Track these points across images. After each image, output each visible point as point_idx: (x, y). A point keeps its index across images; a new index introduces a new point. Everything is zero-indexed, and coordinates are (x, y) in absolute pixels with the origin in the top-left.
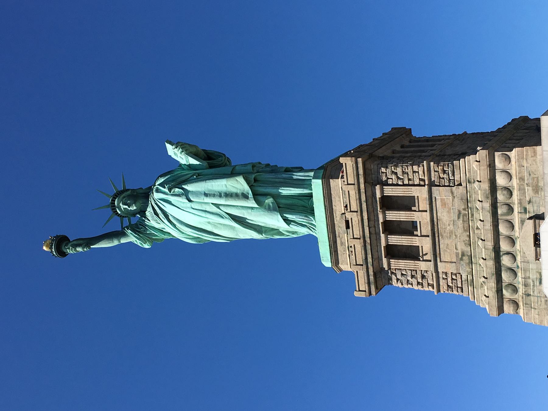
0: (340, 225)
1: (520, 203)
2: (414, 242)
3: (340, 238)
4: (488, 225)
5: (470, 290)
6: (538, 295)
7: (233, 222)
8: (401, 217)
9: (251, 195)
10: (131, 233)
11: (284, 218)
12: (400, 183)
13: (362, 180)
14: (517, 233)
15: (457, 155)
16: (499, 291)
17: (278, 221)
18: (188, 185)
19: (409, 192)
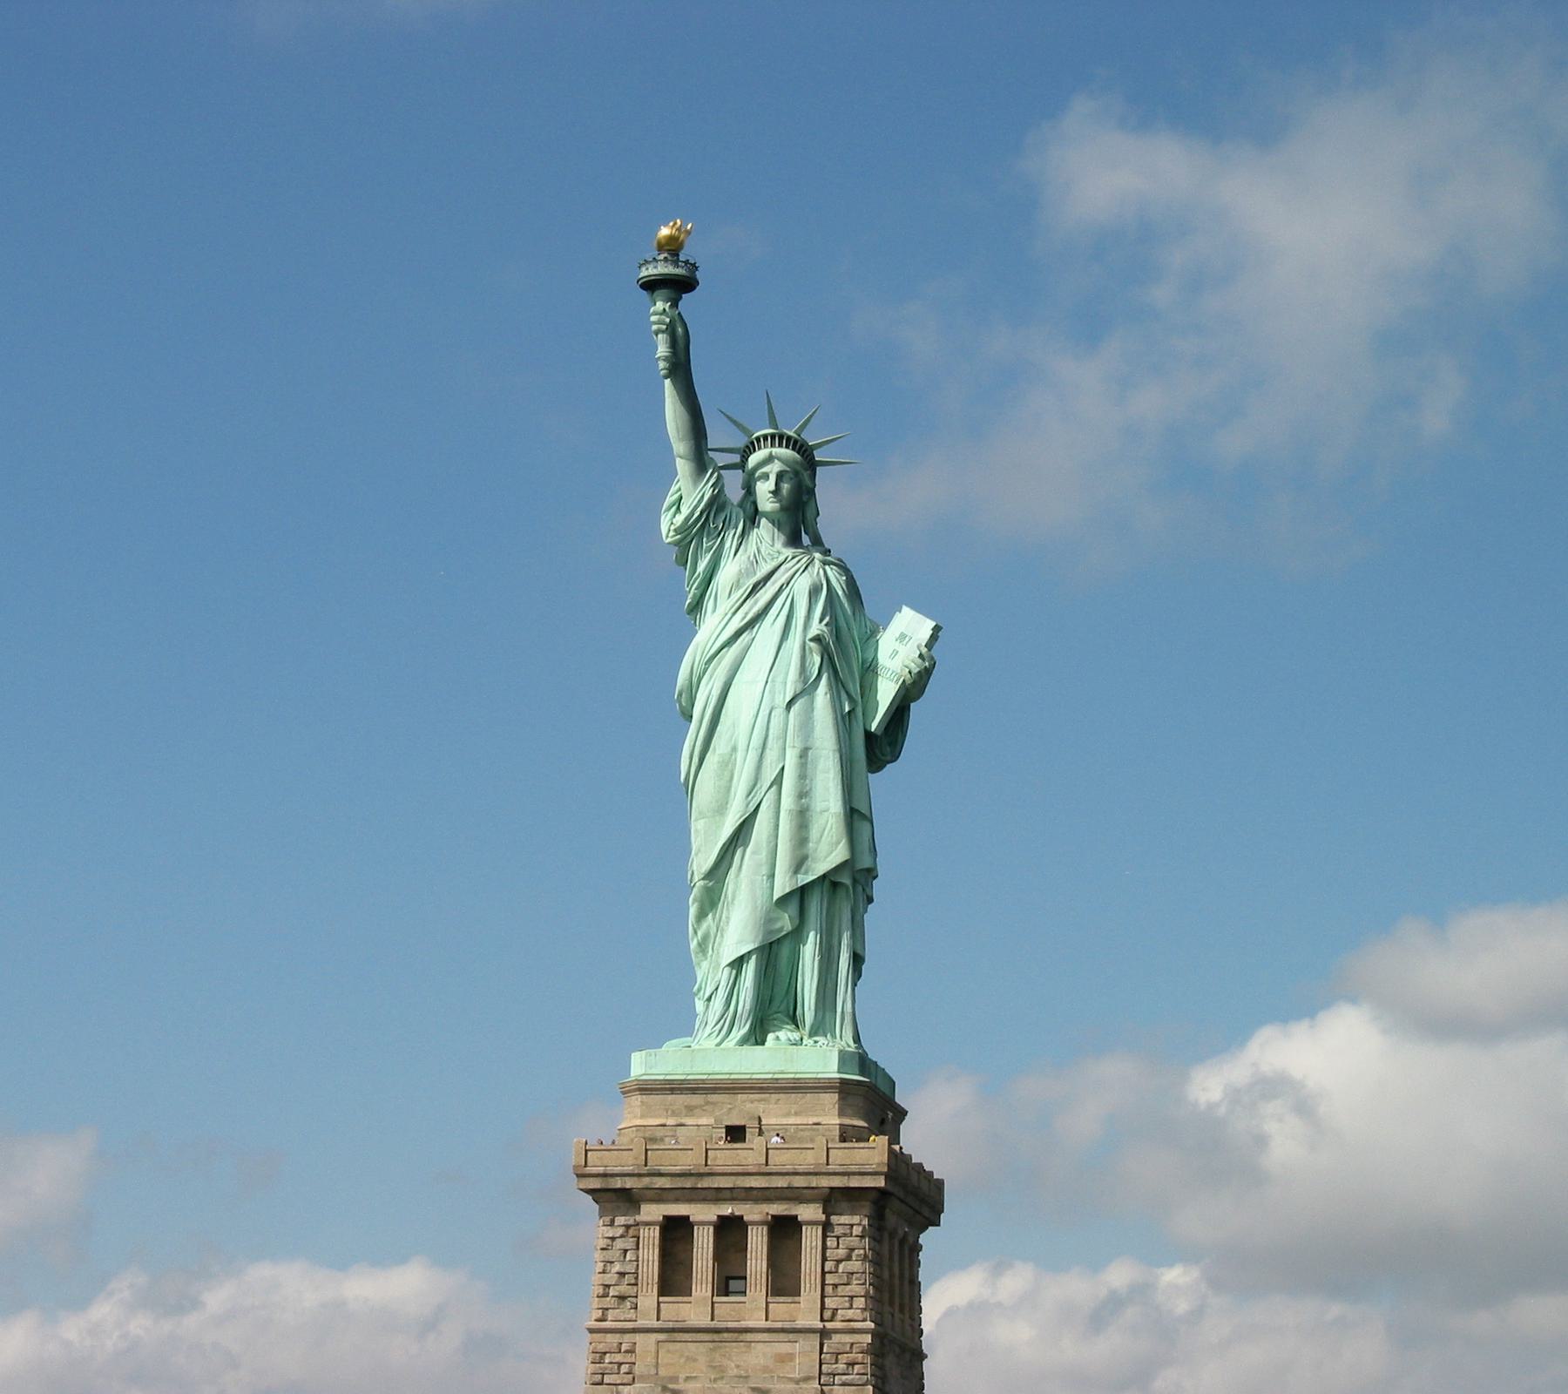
0: (735, 1112)
3: (701, 1106)
7: (736, 822)
8: (754, 1261)
9: (804, 879)
10: (703, 497)
11: (745, 959)
12: (829, 1266)
13: (837, 1182)
15: (883, 1383)
17: (740, 942)
18: (828, 695)
19: (808, 1285)
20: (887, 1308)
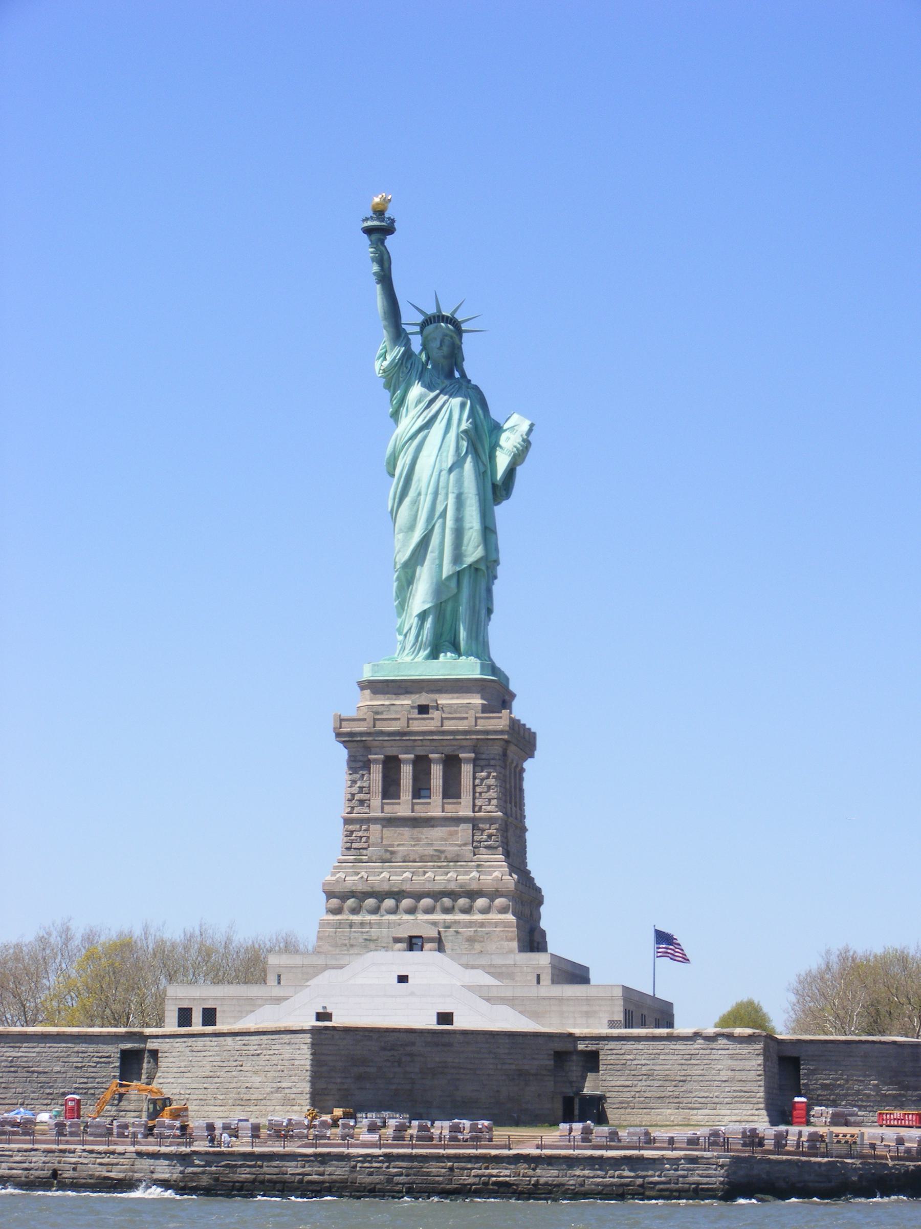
1: (457, 923)
2: (404, 794)
4: (429, 887)
5: (349, 859)
6: (352, 937)
10: (399, 351)
12: (477, 781)
14: (421, 917)
15: (507, 846)
16: (352, 894)
17: (424, 602)
20: (509, 806)
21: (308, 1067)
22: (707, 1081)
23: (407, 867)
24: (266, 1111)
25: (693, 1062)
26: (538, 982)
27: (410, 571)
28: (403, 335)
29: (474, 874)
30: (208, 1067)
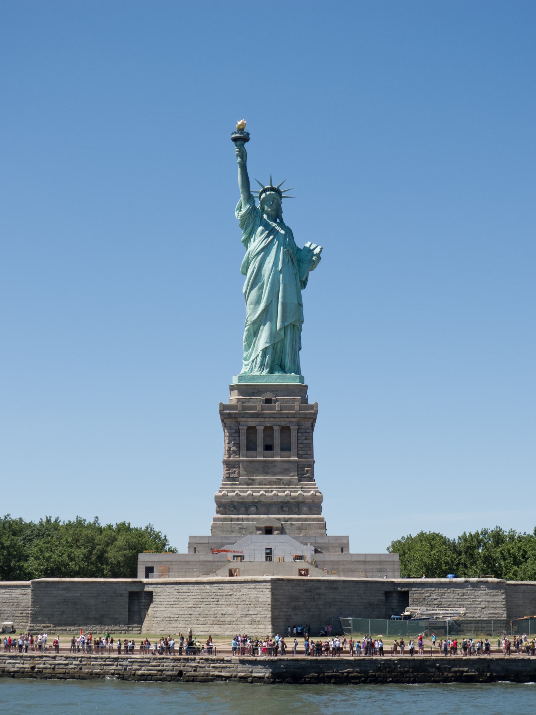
6: (232, 527)
9: (286, 324)
12: (300, 442)
17: (266, 343)
21: (270, 603)
22: (473, 608)
23: (262, 488)
24: (237, 628)
25: (464, 597)
26: (342, 551)
27: (256, 326)
28: (252, 197)
29: (299, 492)
30: (192, 602)
